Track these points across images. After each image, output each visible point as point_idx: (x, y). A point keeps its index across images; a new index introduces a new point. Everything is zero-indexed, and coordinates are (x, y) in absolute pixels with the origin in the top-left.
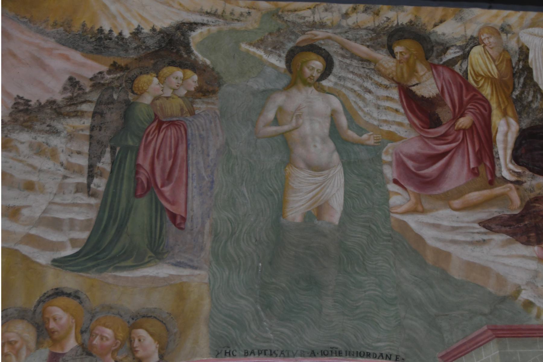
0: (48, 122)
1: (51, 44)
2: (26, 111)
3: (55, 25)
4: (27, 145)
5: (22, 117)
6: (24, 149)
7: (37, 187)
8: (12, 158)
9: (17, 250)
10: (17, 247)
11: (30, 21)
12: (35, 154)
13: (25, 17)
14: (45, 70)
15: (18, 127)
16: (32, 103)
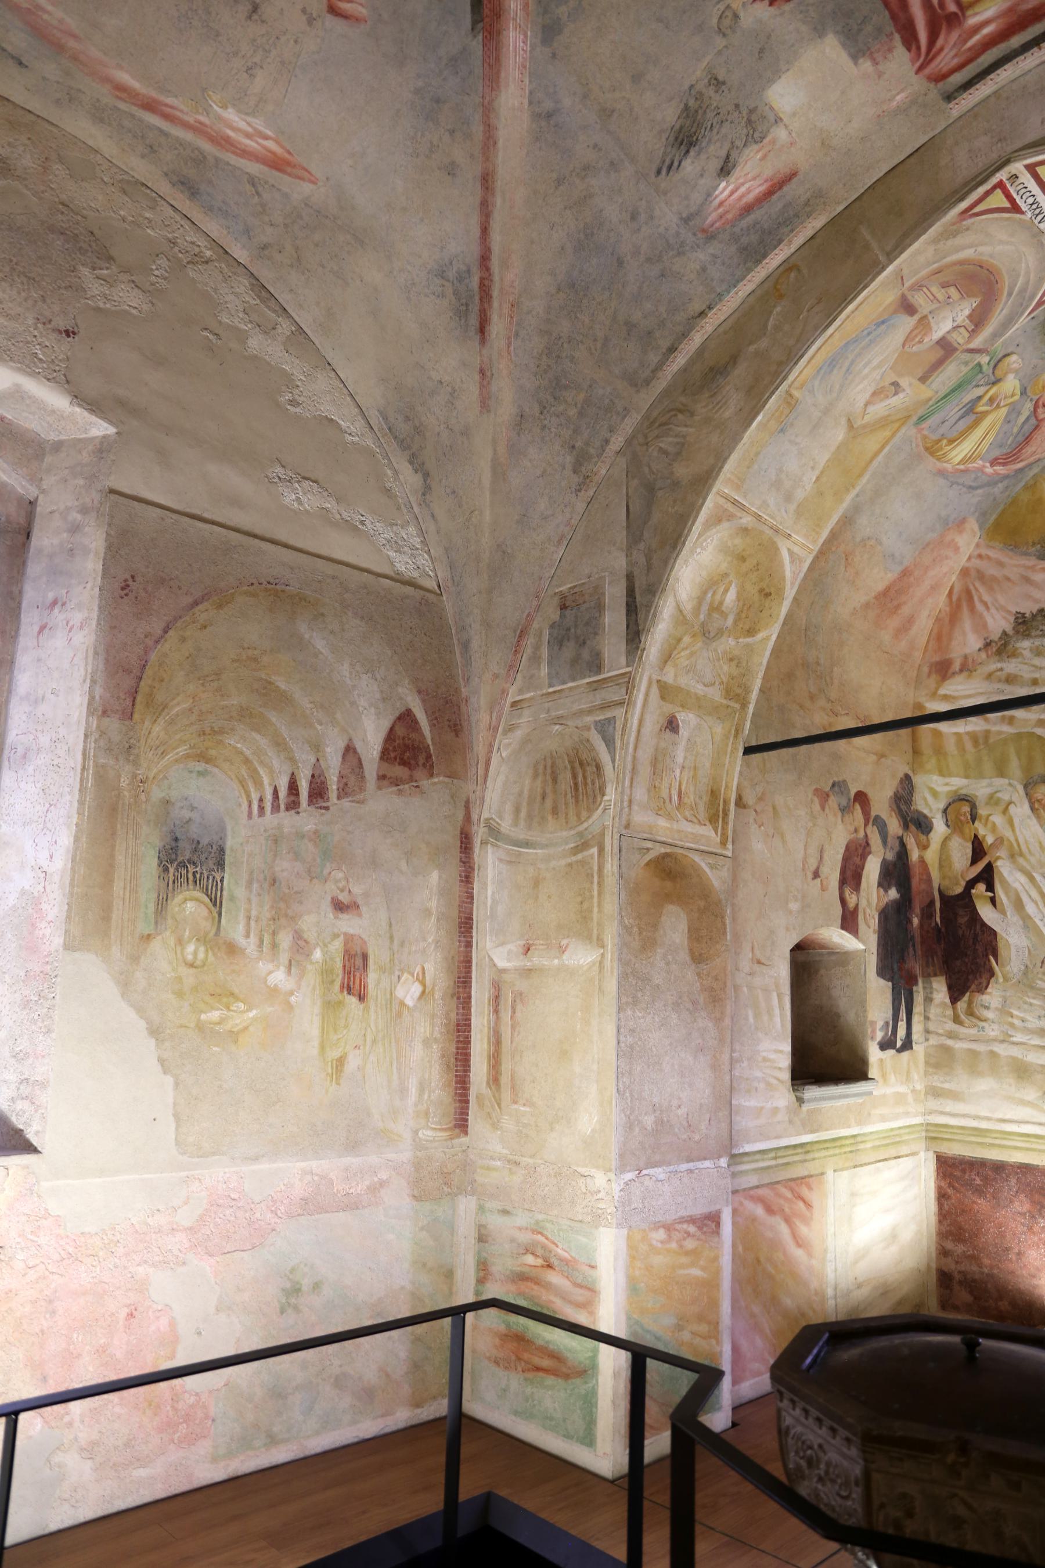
0: (1041, 627)
1: (1032, 561)
2: (1024, 623)
3: (1034, 544)
4: (1028, 650)
5: (1021, 628)
6: (1027, 653)
7: (1040, 681)
8: (1021, 663)
9: (1033, 733)
10: (1033, 731)
11: (1015, 547)
12: (1036, 656)
13: (1011, 545)
14: (1032, 585)
15: (1020, 637)
16: (1027, 615)
